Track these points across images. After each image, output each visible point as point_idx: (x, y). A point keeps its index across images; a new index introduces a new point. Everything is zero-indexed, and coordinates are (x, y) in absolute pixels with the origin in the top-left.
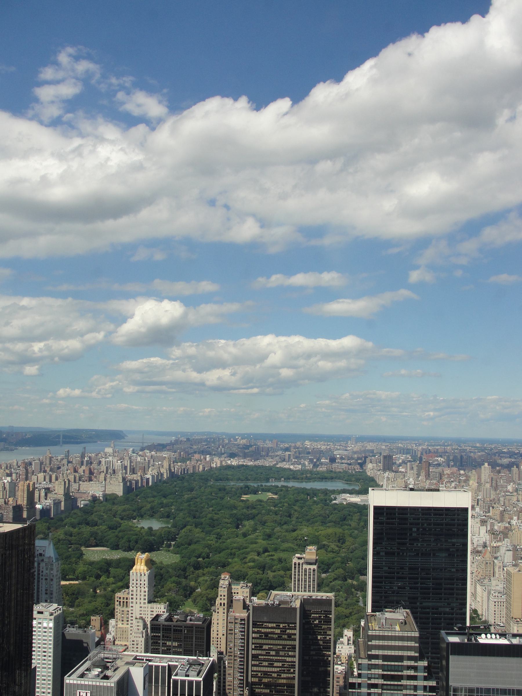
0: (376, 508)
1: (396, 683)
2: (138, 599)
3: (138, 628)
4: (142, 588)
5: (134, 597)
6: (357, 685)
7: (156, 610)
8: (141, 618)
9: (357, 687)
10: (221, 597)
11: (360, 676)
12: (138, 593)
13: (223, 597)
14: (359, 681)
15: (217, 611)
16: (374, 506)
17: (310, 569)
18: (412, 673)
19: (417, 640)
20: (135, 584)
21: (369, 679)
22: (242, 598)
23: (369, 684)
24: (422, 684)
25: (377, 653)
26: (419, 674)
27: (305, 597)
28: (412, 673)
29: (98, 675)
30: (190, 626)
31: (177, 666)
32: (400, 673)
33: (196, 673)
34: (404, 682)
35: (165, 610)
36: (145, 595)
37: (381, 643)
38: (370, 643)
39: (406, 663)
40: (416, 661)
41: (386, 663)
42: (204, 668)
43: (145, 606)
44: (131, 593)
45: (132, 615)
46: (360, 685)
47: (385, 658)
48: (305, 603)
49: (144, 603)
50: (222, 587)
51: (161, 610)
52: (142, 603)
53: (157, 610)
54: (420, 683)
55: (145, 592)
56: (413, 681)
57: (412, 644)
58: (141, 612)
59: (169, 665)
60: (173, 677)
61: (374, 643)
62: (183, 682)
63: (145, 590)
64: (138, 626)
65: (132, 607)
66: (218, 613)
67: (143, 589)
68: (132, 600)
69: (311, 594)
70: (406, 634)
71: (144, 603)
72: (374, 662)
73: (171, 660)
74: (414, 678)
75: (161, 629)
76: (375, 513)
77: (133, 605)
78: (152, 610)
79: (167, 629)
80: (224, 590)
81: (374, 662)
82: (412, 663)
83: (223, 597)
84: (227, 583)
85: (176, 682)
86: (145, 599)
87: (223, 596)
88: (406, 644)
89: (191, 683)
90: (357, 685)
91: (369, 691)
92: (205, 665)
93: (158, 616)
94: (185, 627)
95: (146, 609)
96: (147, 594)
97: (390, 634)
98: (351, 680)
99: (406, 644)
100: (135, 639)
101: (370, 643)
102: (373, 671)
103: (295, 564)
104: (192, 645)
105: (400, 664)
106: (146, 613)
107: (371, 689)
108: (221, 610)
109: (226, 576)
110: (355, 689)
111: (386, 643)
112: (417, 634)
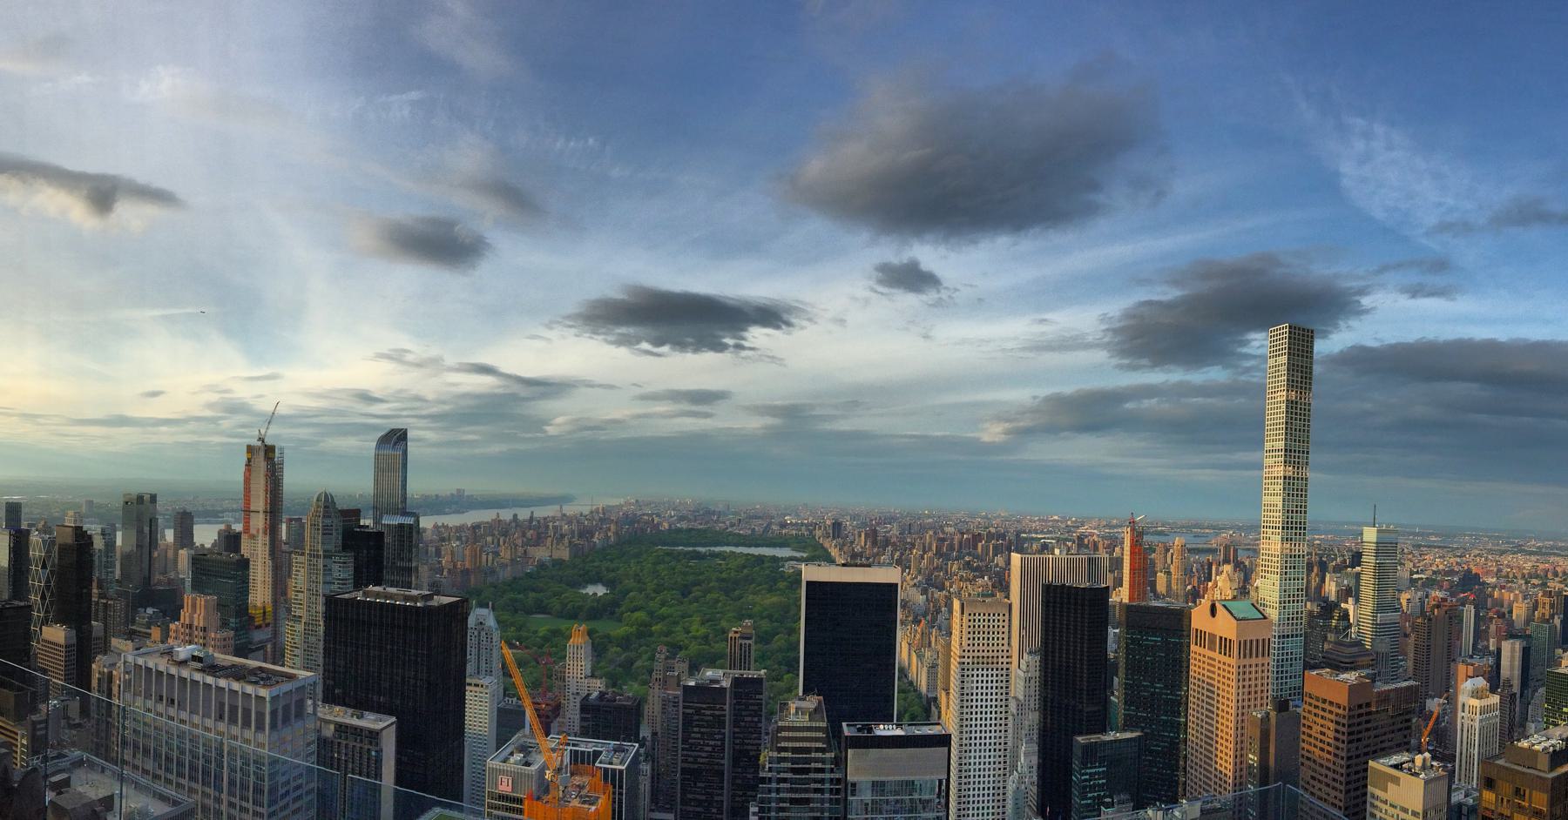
5: (571, 671)
8: (578, 693)
12: (575, 670)
14: (770, 775)
16: (807, 582)
17: (745, 644)
21: (779, 773)
26: (827, 766)
28: (820, 765)
29: (520, 760)
31: (601, 752)
32: (808, 766)
33: (619, 761)
34: (812, 775)
36: (581, 670)
38: (779, 735)
44: (567, 671)
46: (770, 778)
47: (794, 750)
48: (737, 682)
54: (827, 776)
55: (581, 666)
57: (820, 735)
59: (594, 751)
61: (784, 734)
67: (579, 664)
72: (783, 754)
74: (822, 771)
81: (783, 754)
82: (820, 755)
84: (663, 657)
86: (581, 674)
88: (814, 734)
93: (589, 695)
96: (583, 668)
98: (762, 775)
99: (814, 734)
101: (779, 735)
102: (783, 765)
103: (731, 638)
108: (657, 687)
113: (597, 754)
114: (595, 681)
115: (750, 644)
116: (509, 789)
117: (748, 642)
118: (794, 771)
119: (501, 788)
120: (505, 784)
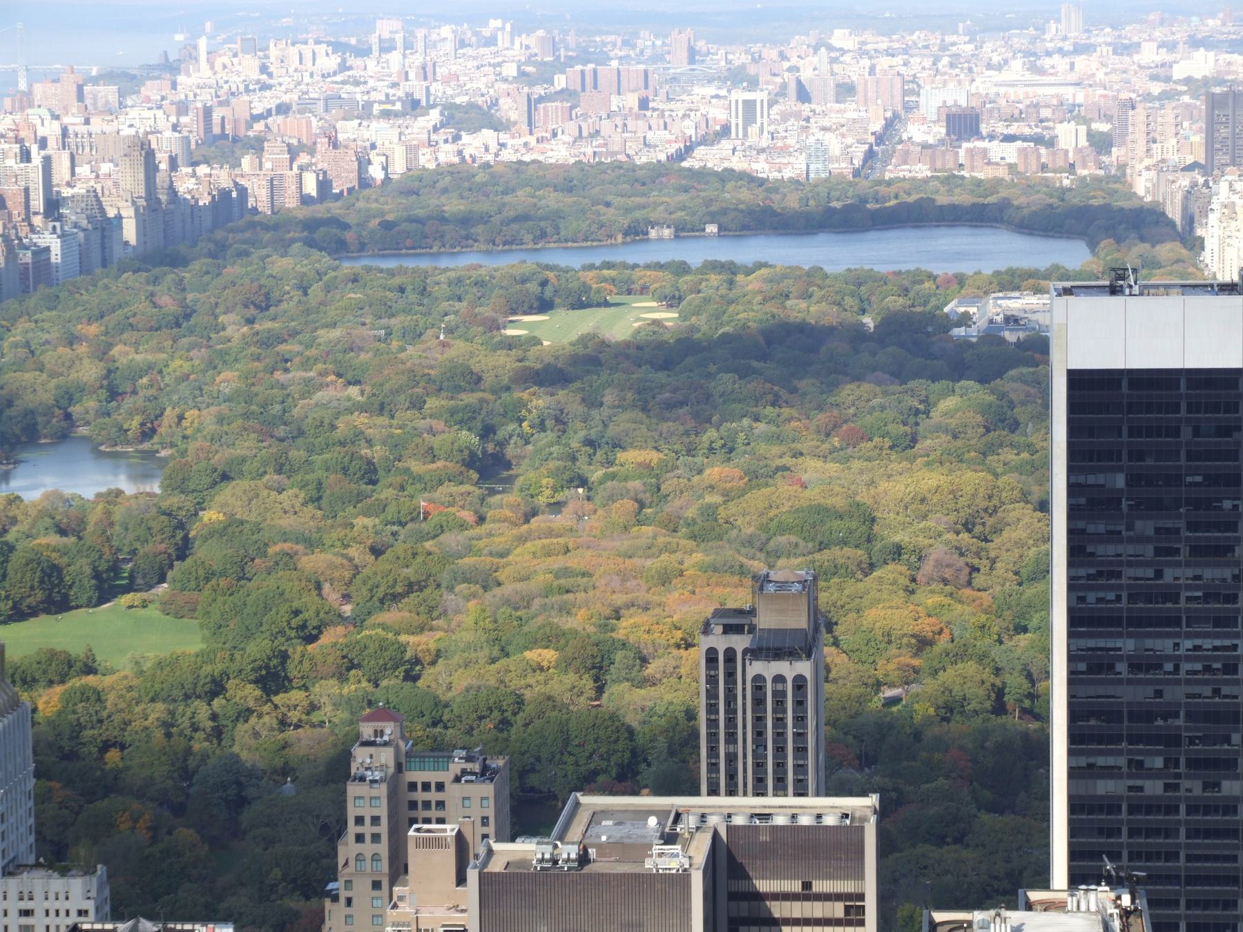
0: (1078, 379)
7: (47, 905)
10: (360, 830)
13: (367, 829)
15: (343, 894)
17: (779, 679)
22: (450, 830)
27: (739, 821)
35: (90, 905)
50: (362, 779)
51: (67, 905)
66: (349, 902)
76: (1074, 407)
80: (374, 793)
83: (367, 829)
84: (386, 757)
87: (368, 821)
114: (57, 884)
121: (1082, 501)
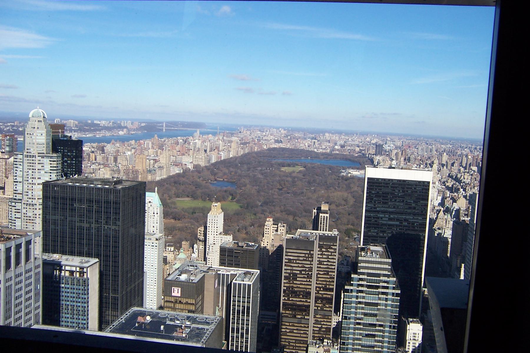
1: (375, 290)
2: (213, 232)
3: (212, 250)
4: (216, 225)
6: (350, 290)
9: (350, 292)
11: (352, 285)
14: (351, 288)
15: (263, 241)
17: (324, 216)
18: (385, 285)
19: (390, 264)
20: (211, 223)
23: (357, 290)
24: (392, 292)
25: (364, 272)
26: (390, 285)
27: (321, 234)
28: (385, 285)
30: (246, 249)
32: (377, 284)
33: (248, 280)
37: (367, 265)
38: (359, 265)
39: (382, 278)
40: (388, 277)
41: (369, 278)
42: (253, 276)
43: (217, 236)
45: (208, 242)
46: (352, 290)
47: (369, 275)
49: (217, 235)
52: (215, 235)
53: (225, 239)
54: (390, 291)
56: (385, 290)
57: (387, 267)
58: (214, 240)
60: (234, 281)
61: (362, 265)
62: (240, 285)
63: (217, 226)
64: (212, 249)
65: (209, 237)
66: (264, 242)
68: (209, 233)
69: (324, 232)
70: (383, 260)
71: (217, 235)
72: (361, 277)
73: (232, 270)
74: (387, 288)
75: (227, 251)
77: (210, 235)
78: (221, 239)
79: (230, 250)
81: (361, 277)
82: (386, 279)
85: (235, 284)
86: (217, 232)
88: (382, 266)
89: (245, 285)
90: (350, 290)
91: (357, 295)
92: (254, 275)
94: (242, 251)
95: (218, 239)
97: (373, 260)
99: (382, 266)
100: (210, 257)
101: (359, 265)
102: (361, 283)
104: (246, 262)
105: (378, 278)
106: (218, 241)
107: (359, 294)
109: (269, 219)
110: (349, 293)
111: (370, 265)
112: (390, 261)
113: (234, 276)
114: (226, 236)
115: (327, 217)
116: (179, 295)
117: (326, 215)
118: (369, 287)
119: (173, 294)
120: (176, 291)
121: (368, 195)
